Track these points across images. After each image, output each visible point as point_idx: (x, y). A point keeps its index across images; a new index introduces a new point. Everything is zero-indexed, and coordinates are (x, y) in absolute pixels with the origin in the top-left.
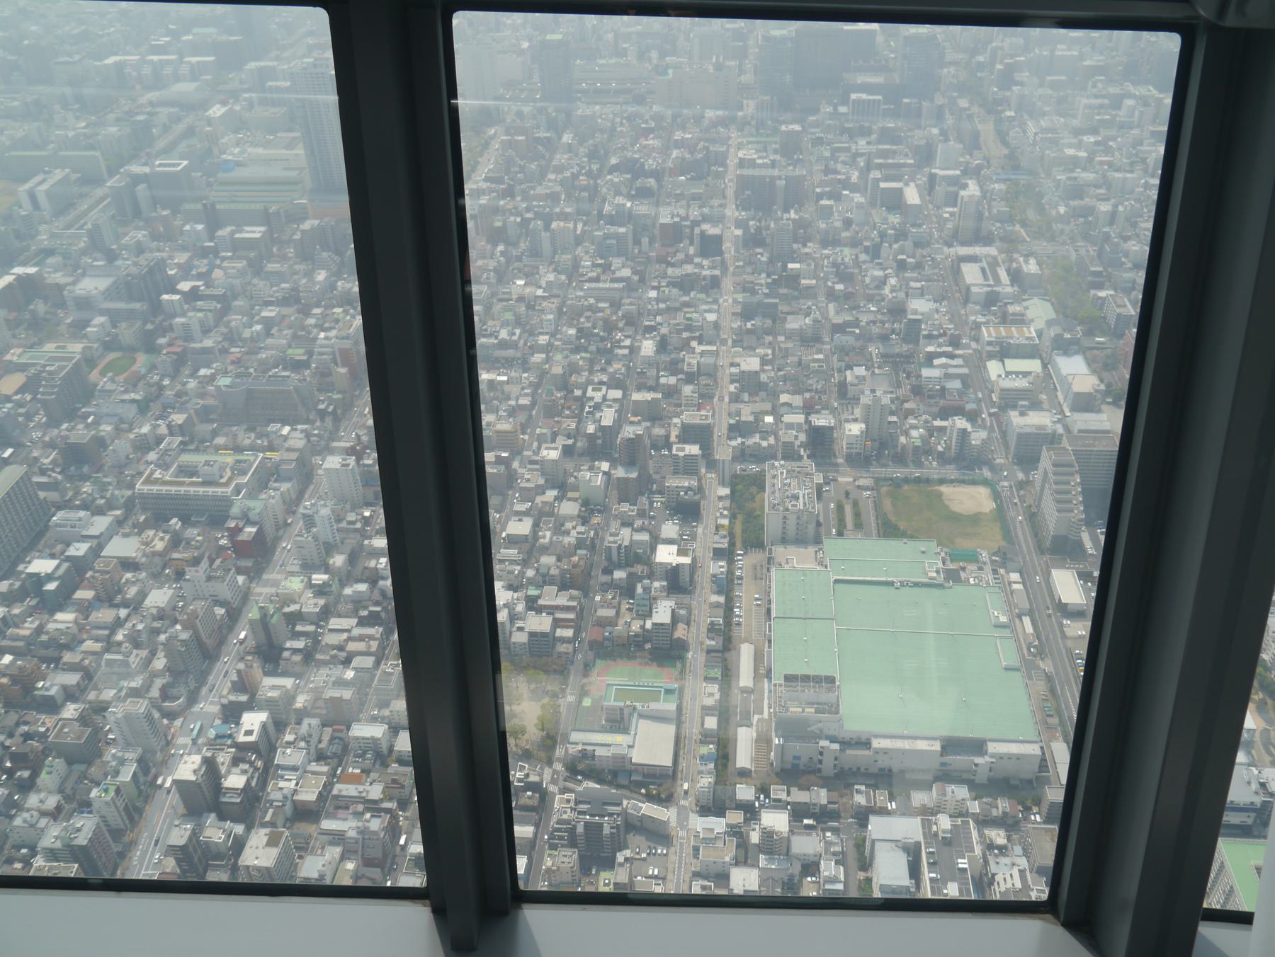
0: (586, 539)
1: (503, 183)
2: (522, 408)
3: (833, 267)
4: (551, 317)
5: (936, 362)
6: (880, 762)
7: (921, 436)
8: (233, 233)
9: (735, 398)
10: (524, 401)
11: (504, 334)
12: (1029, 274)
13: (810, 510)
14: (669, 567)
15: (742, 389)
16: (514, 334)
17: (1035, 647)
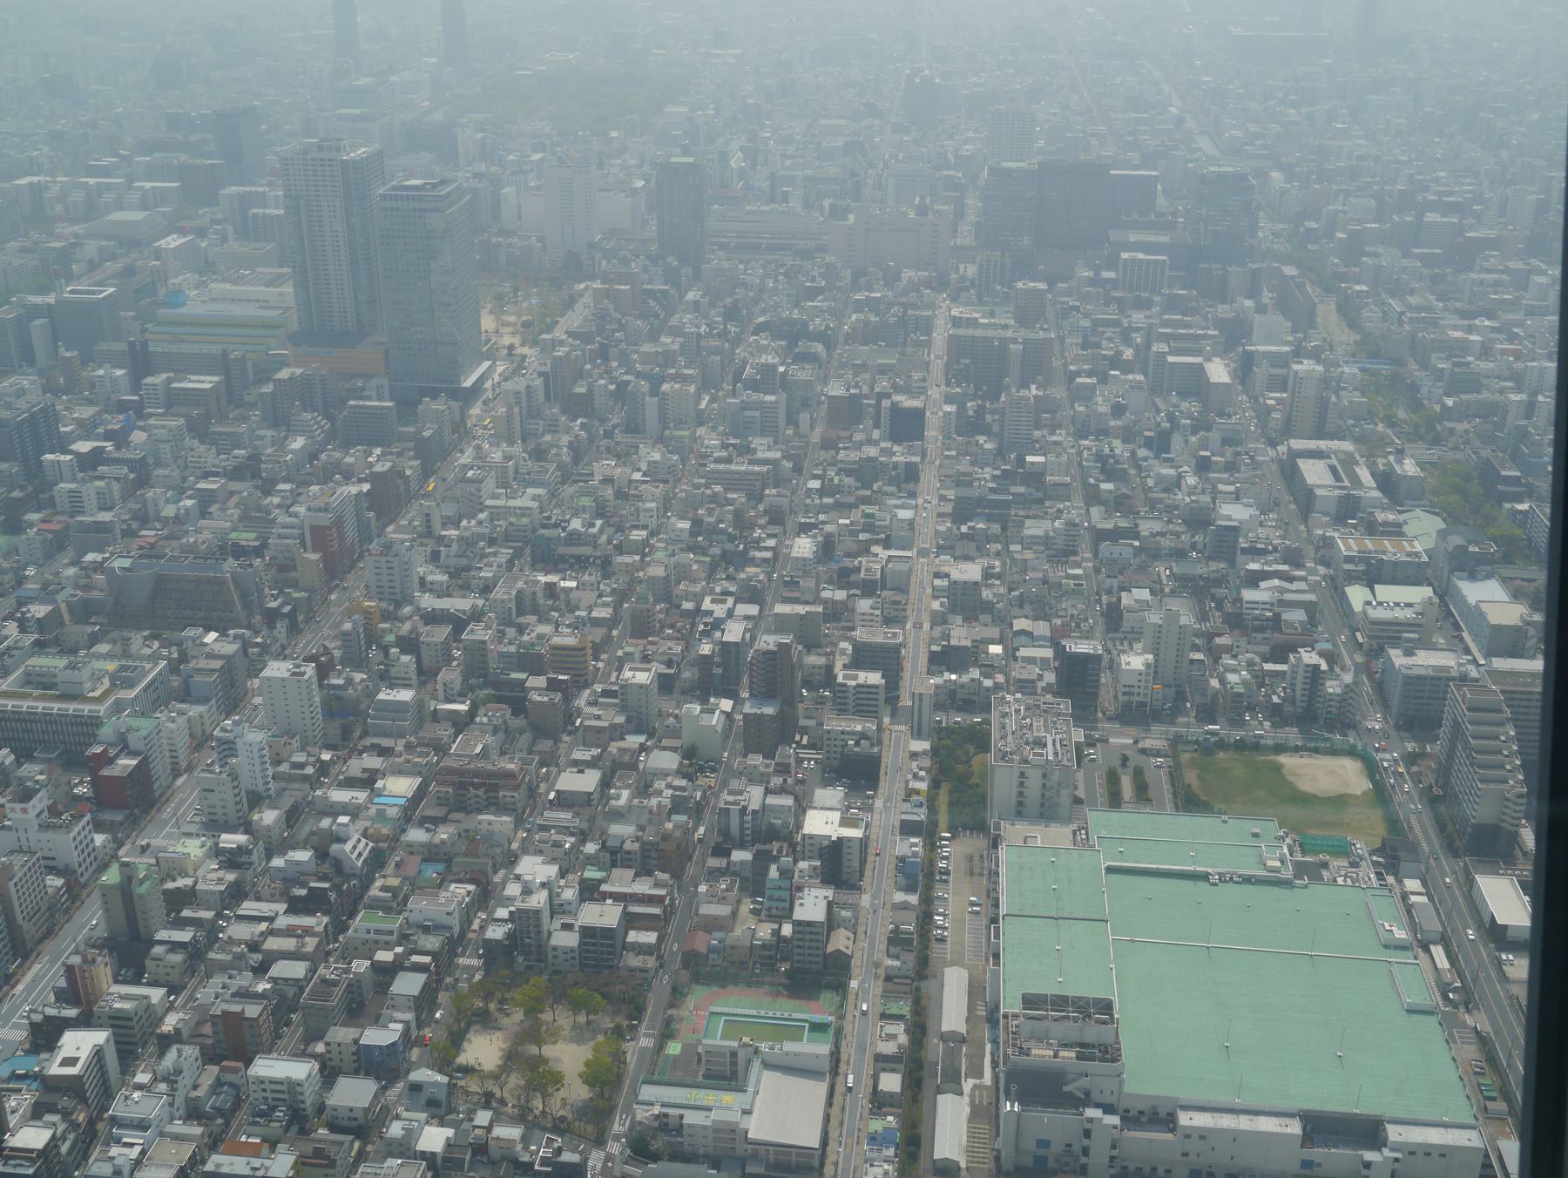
0: (687, 799)
1: (592, 342)
2: (597, 623)
3: (1096, 461)
4: (653, 505)
5: (1263, 584)
6: (1192, 1157)
7: (1244, 682)
8: (170, 381)
9: (939, 619)
10: (602, 613)
11: (576, 524)
12: (1405, 477)
13: (1065, 762)
14: (826, 843)
15: (953, 608)
16: (592, 525)
17: (1455, 990)
